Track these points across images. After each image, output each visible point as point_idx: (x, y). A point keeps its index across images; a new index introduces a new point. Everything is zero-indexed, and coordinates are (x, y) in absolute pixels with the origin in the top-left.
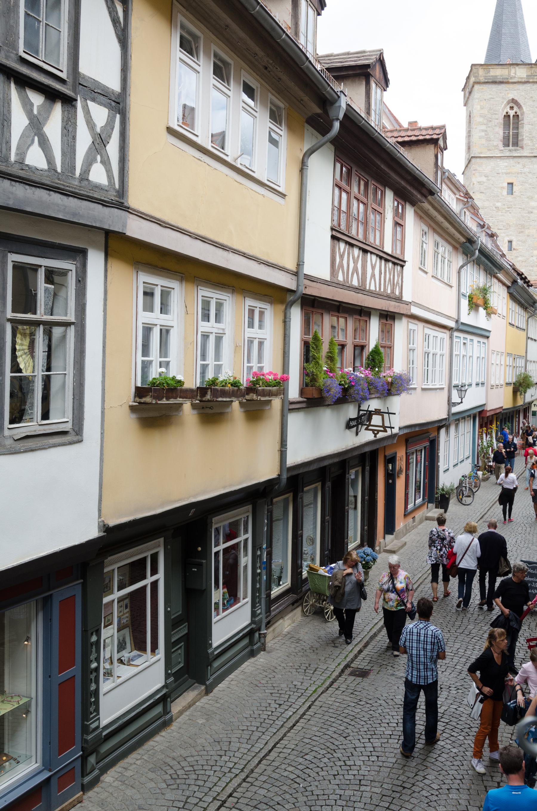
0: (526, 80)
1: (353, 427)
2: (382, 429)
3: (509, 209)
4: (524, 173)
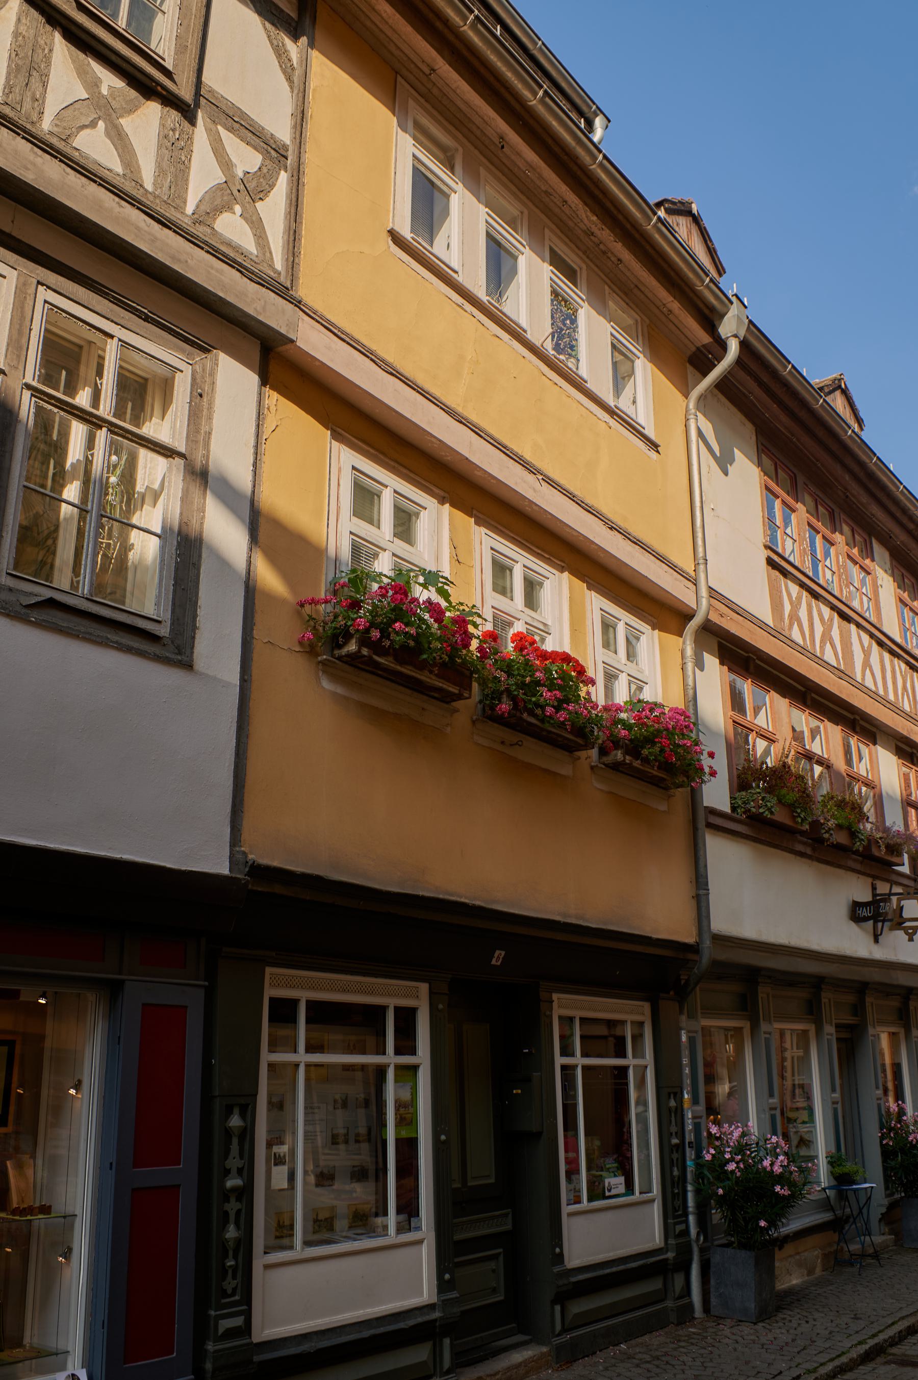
1: (866, 919)
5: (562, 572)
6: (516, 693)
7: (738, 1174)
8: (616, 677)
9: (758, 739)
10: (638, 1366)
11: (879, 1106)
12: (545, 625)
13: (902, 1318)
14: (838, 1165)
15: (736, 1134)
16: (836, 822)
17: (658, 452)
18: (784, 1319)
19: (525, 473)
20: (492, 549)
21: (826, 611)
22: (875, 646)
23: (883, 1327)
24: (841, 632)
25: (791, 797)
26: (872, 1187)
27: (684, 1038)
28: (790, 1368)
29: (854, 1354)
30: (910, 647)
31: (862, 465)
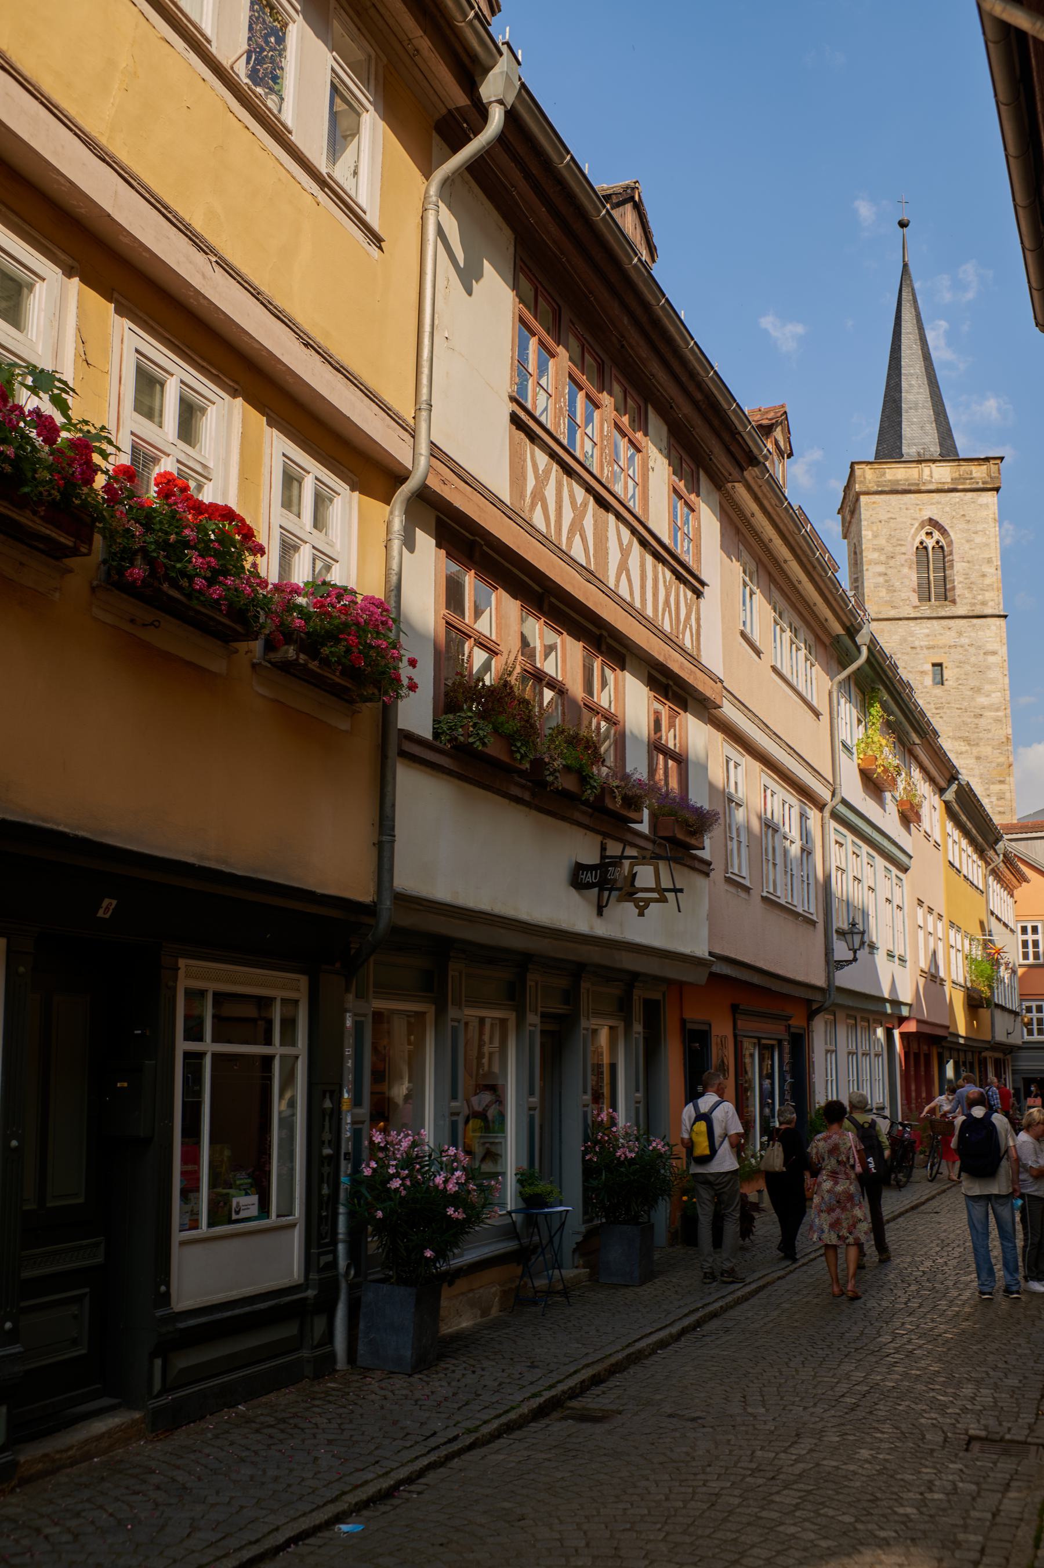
0: (951, 486)
1: (589, 886)
2: (655, 895)
3: (938, 711)
4: (962, 647)
5: (234, 397)
6: (155, 555)
7: (404, 1193)
8: (296, 548)
9: (476, 649)
10: (257, 1431)
11: (585, 1114)
12: (205, 466)
13: (587, 1366)
14: (530, 1185)
15: (405, 1144)
16: (564, 763)
17: (380, 248)
18: (447, 1369)
19: (193, 250)
20: (137, 351)
21: (580, 493)
22: (636, 544)
23: (563, 1377)
24: (595, 521)
25: (512, 726)
26: (567, 1211)
27: (349, 1023)
28: (447, 1427)
29: (525, 1409)
30: (679, 551)
31: (647, 307)
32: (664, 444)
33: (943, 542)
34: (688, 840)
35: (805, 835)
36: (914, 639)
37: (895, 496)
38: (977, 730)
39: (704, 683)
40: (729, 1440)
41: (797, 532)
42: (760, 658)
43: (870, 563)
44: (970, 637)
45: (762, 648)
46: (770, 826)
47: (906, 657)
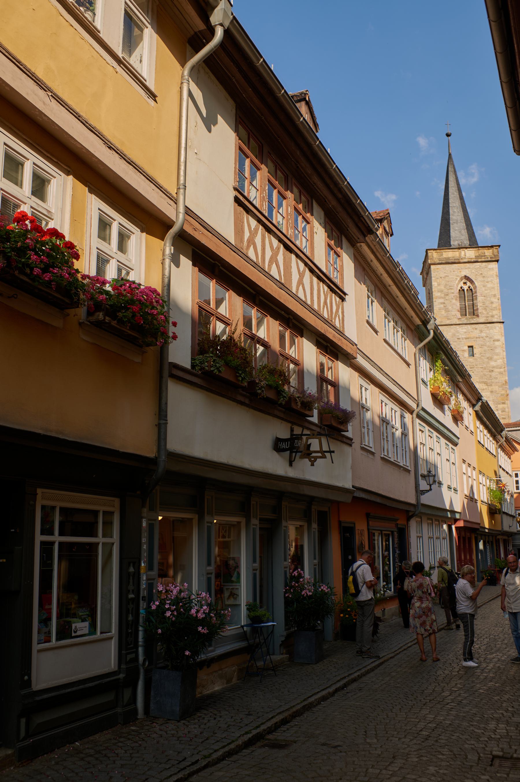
0: (475, 260)
1: (284, 450)
2: (320, 455)
3: (471, 369)
4: (482, 338)
5: (68, 175)
6: (10, 254)
7: (174, 619)
8: (108, 261)
9: (217, 322)
10: (82, 759)
11: (285, 572)
12: (49, 212)
13: (280, 713)
14: (253, 611)
15: (175, 592)
16: (267, 383)
17: (155, 101)
18: (200, 717)
19: (37, 88)
20: (5, 144)
21: (275, 242)
22: (307, 271)
23: (265, 721)
24: (284, 258)
25: (237, 362)
26: (274, 625)
27: (144, 524)
28: (193, 754)
29: (240, 742)
30: (332, 277)
31: (310, 146)
32: (322, 221)
33: (472, 287)
34: (339, 426)
35: (404, 426)
36: (459, 334)
37: (448, 265)
38: (491, 378)
39: (347, 345)
40: (354, 761)
41: (395, 270)
42: (377, 334)
43: (437, 297)
44: (486, 333)
45: (378, 330)
46: (384, 421)
47: (455, 343)
